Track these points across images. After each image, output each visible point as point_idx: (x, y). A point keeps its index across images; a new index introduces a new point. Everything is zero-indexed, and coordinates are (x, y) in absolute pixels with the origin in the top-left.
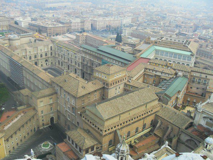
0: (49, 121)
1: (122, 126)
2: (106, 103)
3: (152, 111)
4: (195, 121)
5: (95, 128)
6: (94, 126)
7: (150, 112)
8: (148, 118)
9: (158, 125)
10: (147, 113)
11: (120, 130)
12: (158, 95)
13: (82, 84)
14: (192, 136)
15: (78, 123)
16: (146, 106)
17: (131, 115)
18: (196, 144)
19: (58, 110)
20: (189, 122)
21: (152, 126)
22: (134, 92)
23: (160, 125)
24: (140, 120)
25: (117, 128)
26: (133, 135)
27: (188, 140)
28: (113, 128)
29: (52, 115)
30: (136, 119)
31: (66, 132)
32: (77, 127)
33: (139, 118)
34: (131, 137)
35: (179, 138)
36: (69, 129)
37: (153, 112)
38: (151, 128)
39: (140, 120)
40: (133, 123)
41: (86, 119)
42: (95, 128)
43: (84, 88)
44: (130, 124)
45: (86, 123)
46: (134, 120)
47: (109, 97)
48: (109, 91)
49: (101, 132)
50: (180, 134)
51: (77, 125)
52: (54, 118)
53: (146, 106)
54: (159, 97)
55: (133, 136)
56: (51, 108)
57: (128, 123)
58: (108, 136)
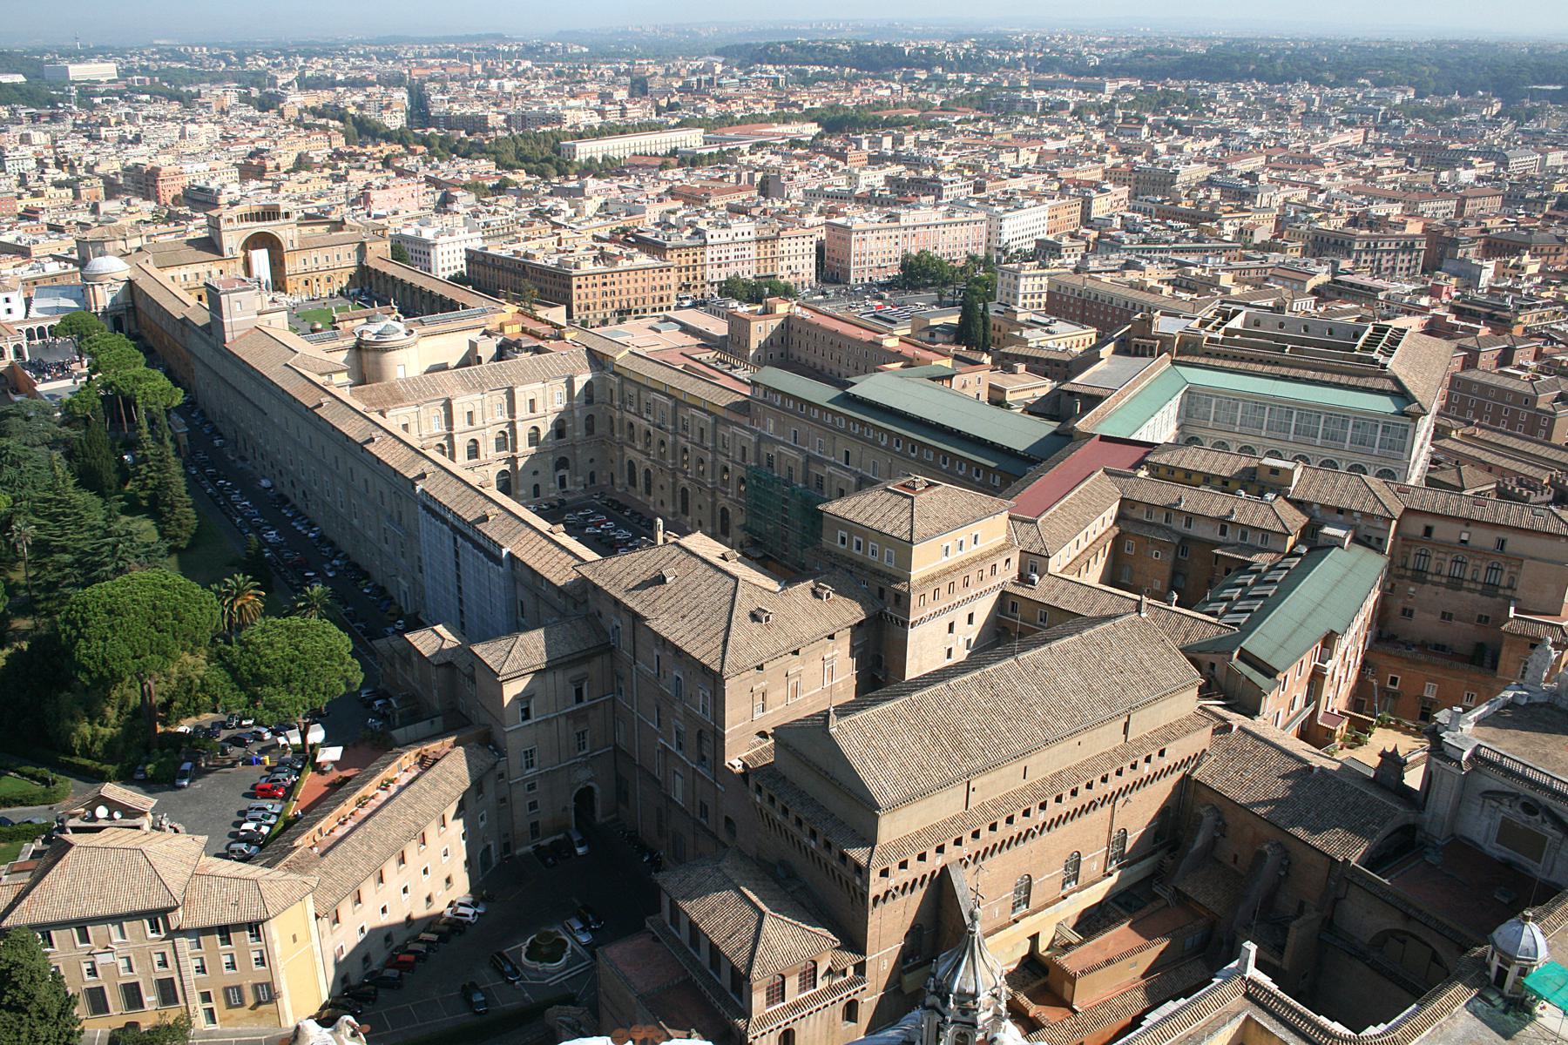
0: (565, 809)
1: (979, 846)
2: (890, 705)
3: (1162, 753)
4: (1427, 816)
5: (824, 854)
6: (820, 840)
7: (1148, 760)
8: (1134, 796)
9: (1199, 841)
10: (1134, 767)
11: (972, 868)
12: (1201, 657)
13: (757, 595)
14: (1410, 911)
15: (728, 820)
16: (1126, 725)
17: (1035, 776)
18: (1435, 958)
19: (616, 746)
20: (1390, 826)
21: (1161, 847)
22: (1054, 645)
23: (1213, 843)
24: (1093, 805)
25: (952, 853)
26: (1049, 897)
27: (1385, 937)
28: (931, 853)
29: (583, 775)
30: (1069, 804)
31: (659, 878)
32: (725, 846)
33: (1085, 796)
34: (1035, 912)
35: (1331, 919)
36: (680, 859)
37: (1166, 762)
38: (1159, 854)
39: (1093, 805)
40: (1046, 827)
41: (772, 800)
42: (824, 854)
43: (767, 619)
44: (1028, 834)
45: (772, 822)
46: (1054, 810)
47: (911, 673)
48: (912, 634)
49: (858, 882)
50: (1337, 900)
51: (723, 836)
52: (597, 791)
53: (1126, 725)
54: (1206, 669)
55: (1047, 906)
56: (581, 735)
57: (1021, 824)
58: (900, 899)
